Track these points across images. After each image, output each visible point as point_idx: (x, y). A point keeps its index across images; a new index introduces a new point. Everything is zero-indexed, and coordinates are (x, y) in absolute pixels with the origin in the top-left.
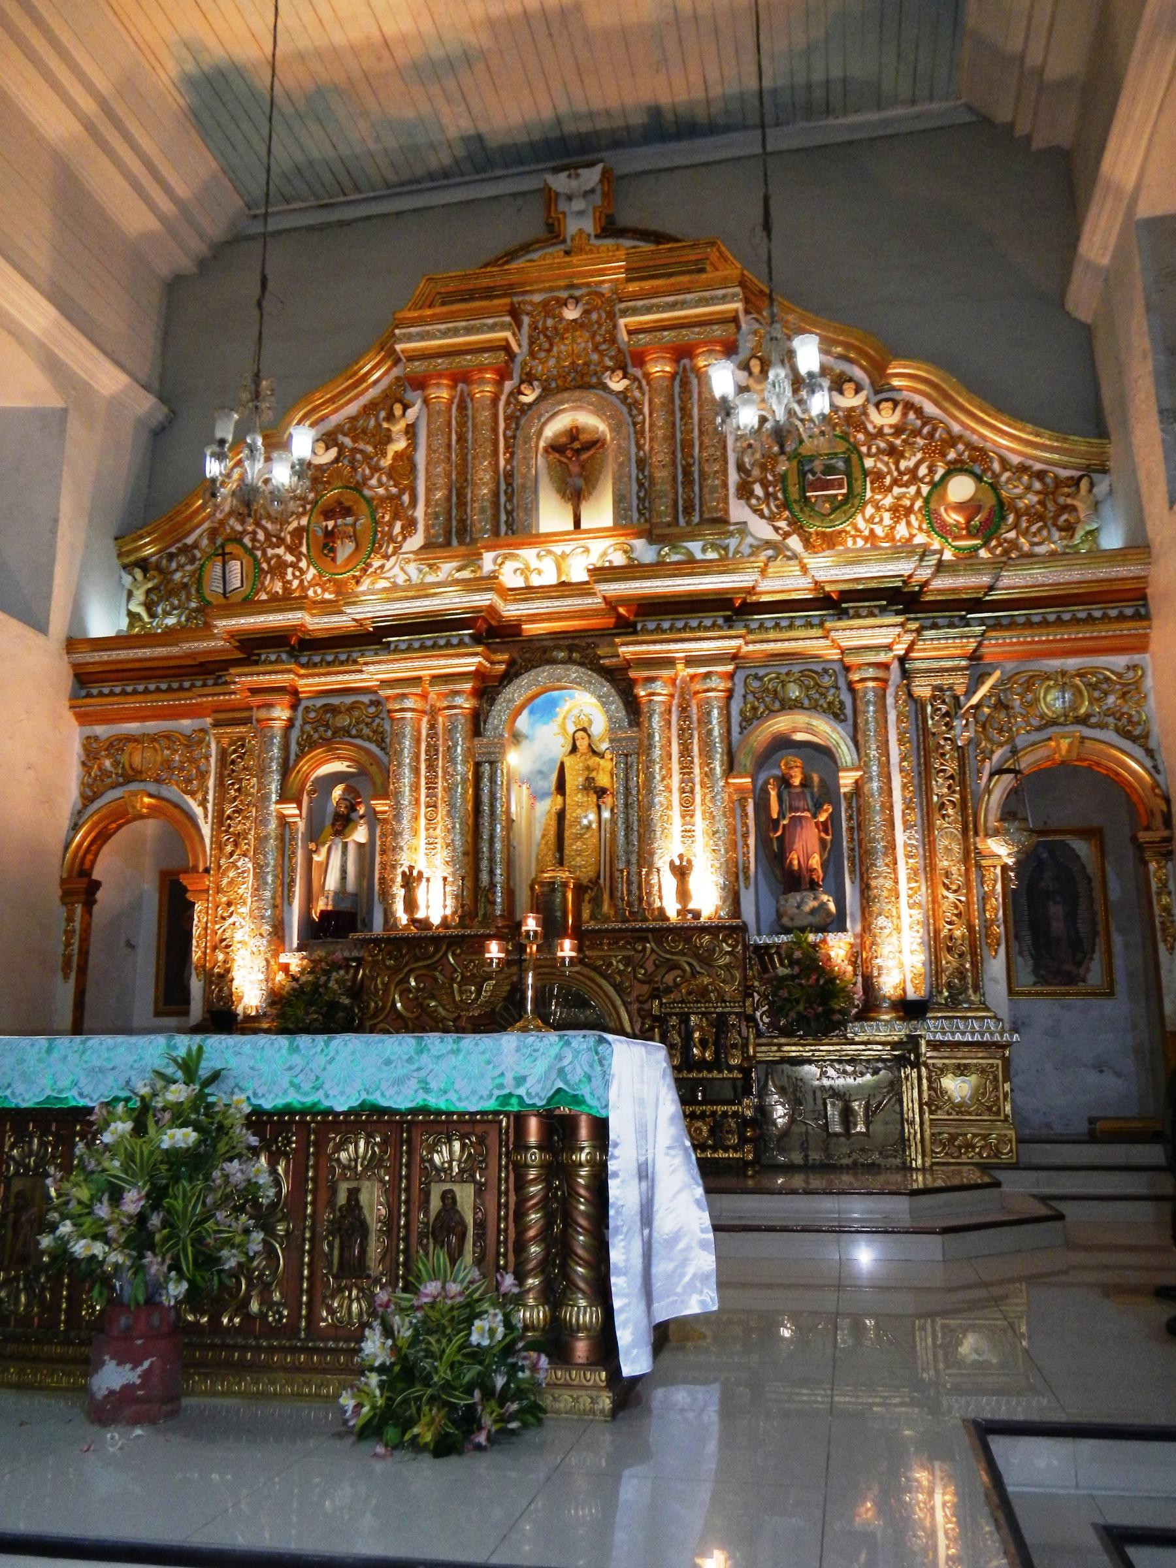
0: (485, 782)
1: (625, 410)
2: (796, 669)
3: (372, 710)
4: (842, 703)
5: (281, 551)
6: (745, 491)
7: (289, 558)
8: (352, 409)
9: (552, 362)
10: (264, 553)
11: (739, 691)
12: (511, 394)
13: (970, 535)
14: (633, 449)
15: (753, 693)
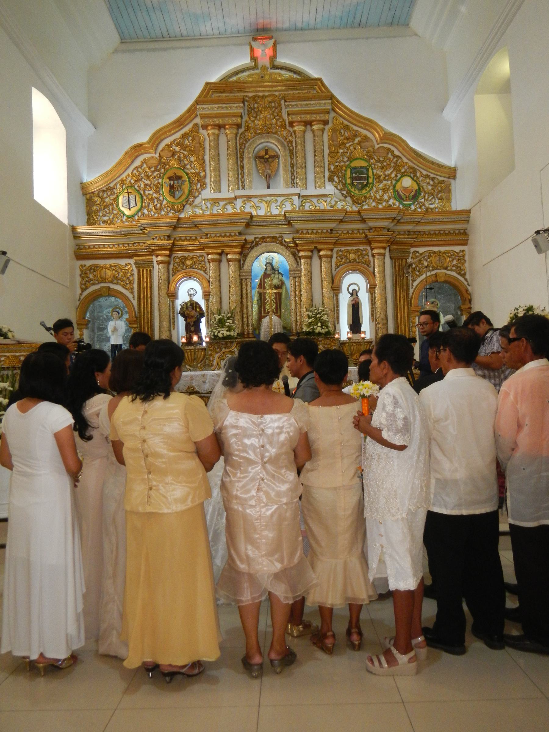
0: (244, 286)
1: (286, 143)
2: (354, 248)
3: (201, 258)
4: (369, 261)
5: (151, 192)
6: (331, 179)
7: (155, 195)
8: (178, 135)
9: (257, 122)
10: (145, 193)
11: (335, 256)
12: (241, 134)
13: (410, 200)
14: (289, 159)
15: (340, 257)
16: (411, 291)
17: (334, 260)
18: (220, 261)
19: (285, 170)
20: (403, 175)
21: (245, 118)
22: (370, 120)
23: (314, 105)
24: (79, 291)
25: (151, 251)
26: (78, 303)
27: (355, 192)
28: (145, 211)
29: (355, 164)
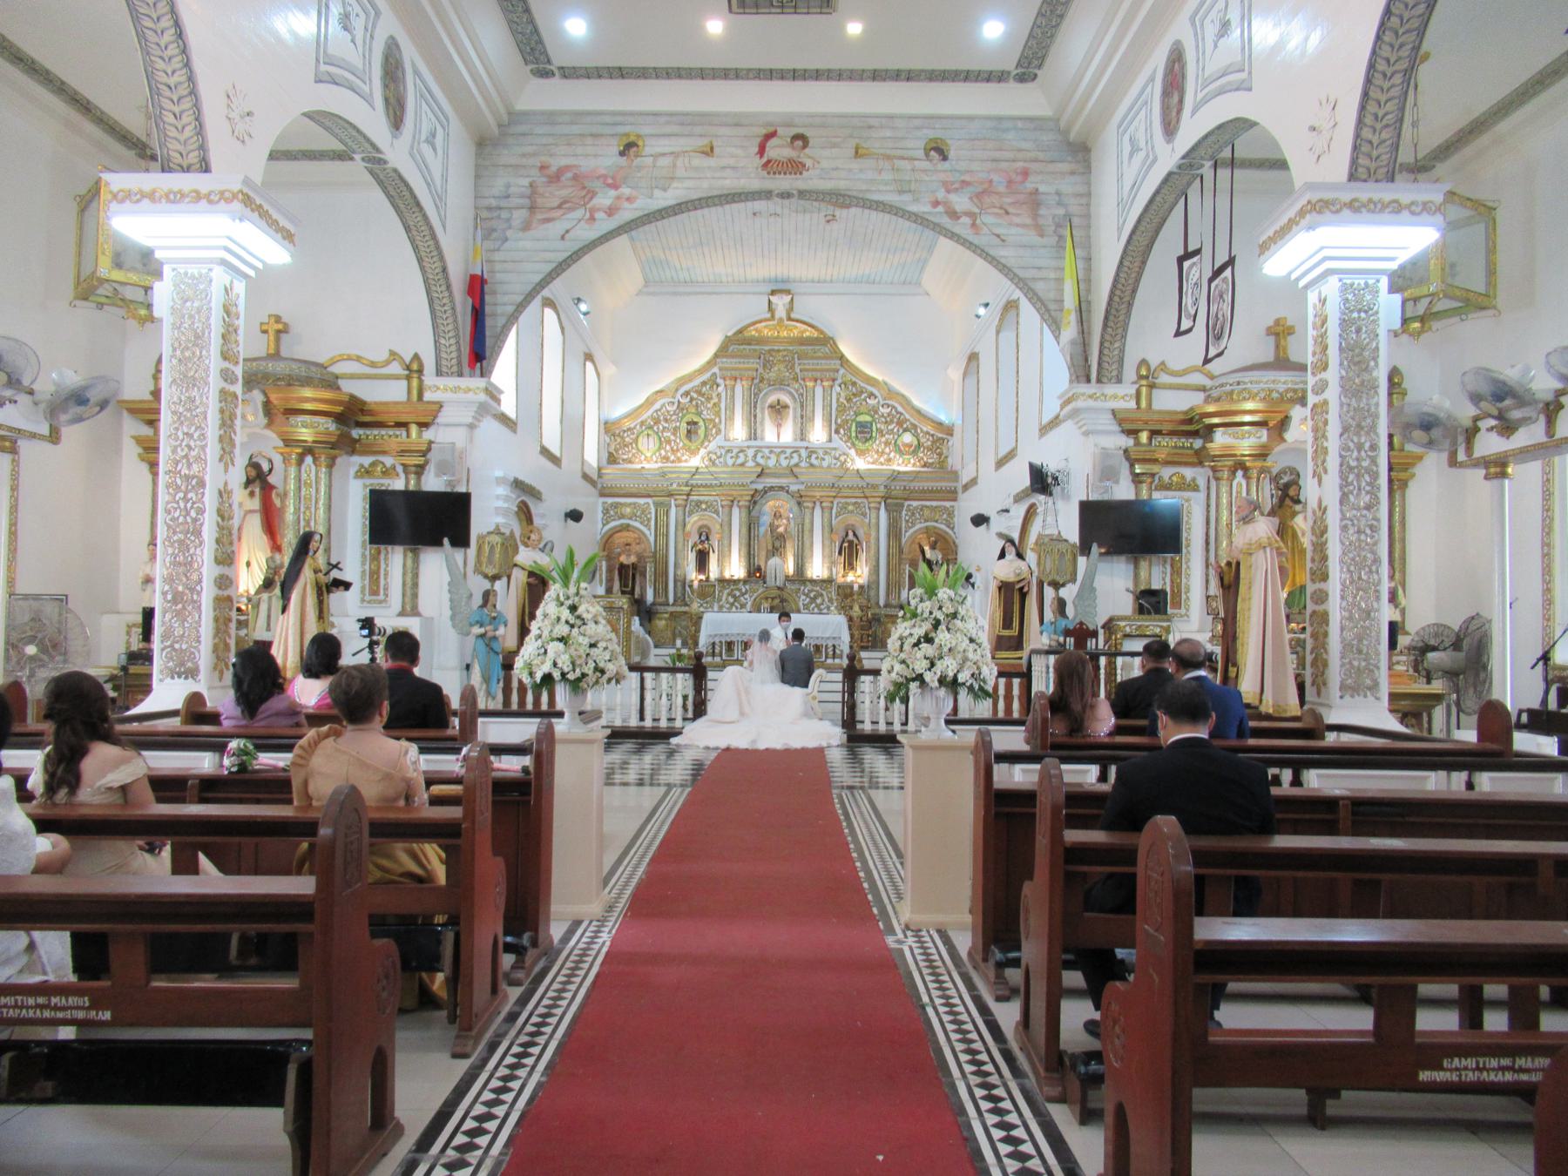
6: (837, 432)
8: (697, 382)
16: (904, 540)
17: (834, 511)
18: (731, 507)
19: (794, 421)
20: (905, 430)
21: (761, 370)
22: (876, 380)
23: (824, 364)
24: (600, 526)
25: (670, 495)
26: (599, 537)
27: (860, 445)
28: (663, 452)
29: (862, 418)
